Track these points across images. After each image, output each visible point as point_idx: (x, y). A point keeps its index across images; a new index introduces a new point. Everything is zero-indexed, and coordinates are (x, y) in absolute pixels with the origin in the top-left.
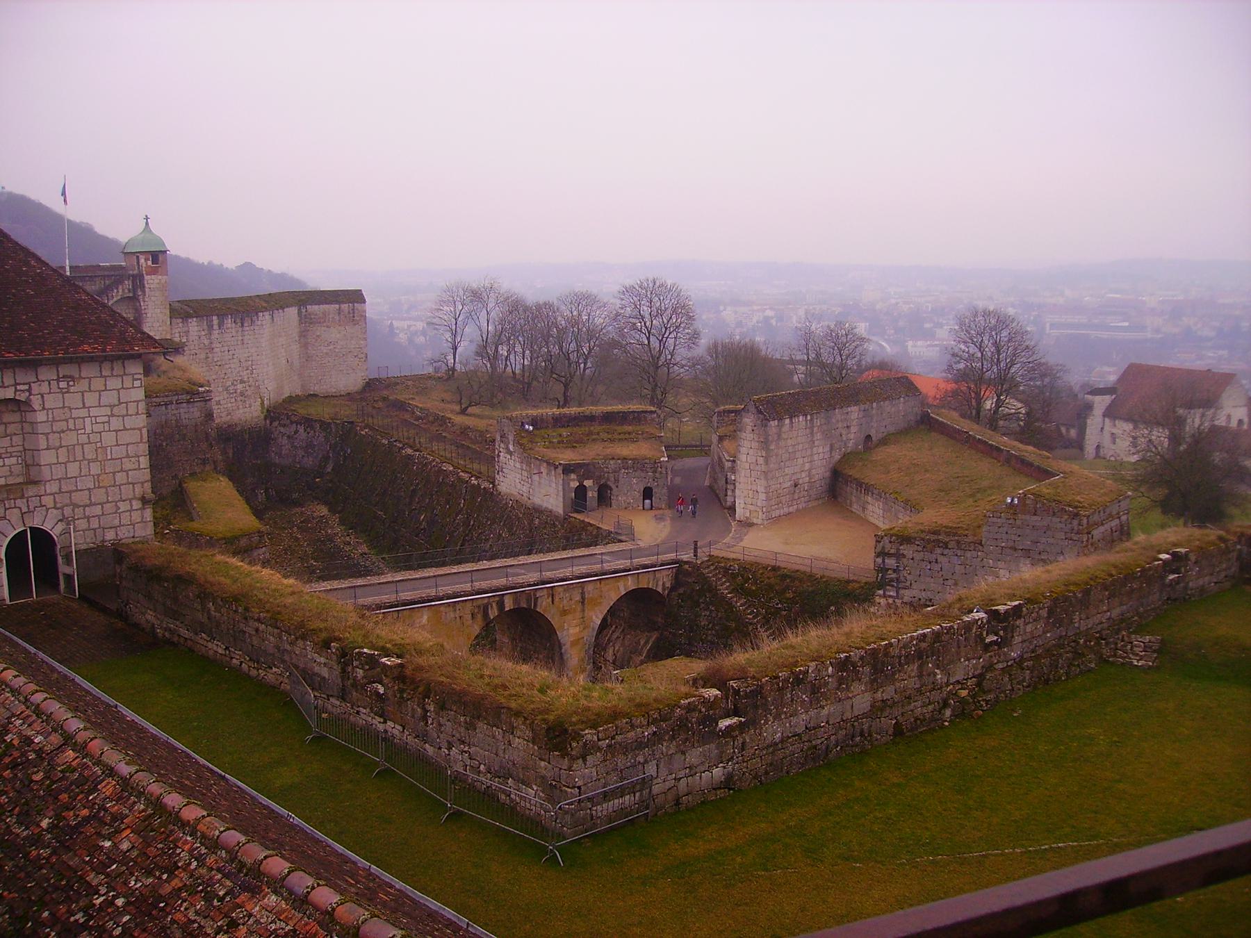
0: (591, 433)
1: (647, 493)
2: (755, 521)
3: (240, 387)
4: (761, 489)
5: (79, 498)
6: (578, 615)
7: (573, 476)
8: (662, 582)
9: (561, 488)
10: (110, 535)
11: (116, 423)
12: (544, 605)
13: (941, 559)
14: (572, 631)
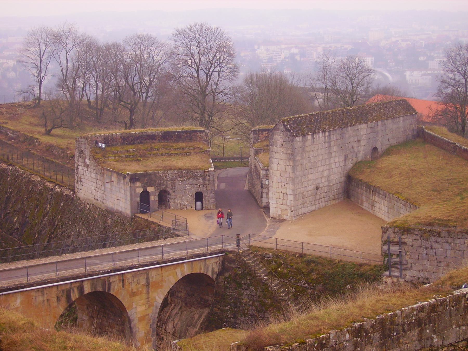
0: (152, 149)
1: (199, 197)
2: (285, 217)
4: (290, 192)
6: (144, 296)
7: (138, 184)
8: (211, 268)
9: (128, 193)
12: (116, 289)
13: (435, 245)
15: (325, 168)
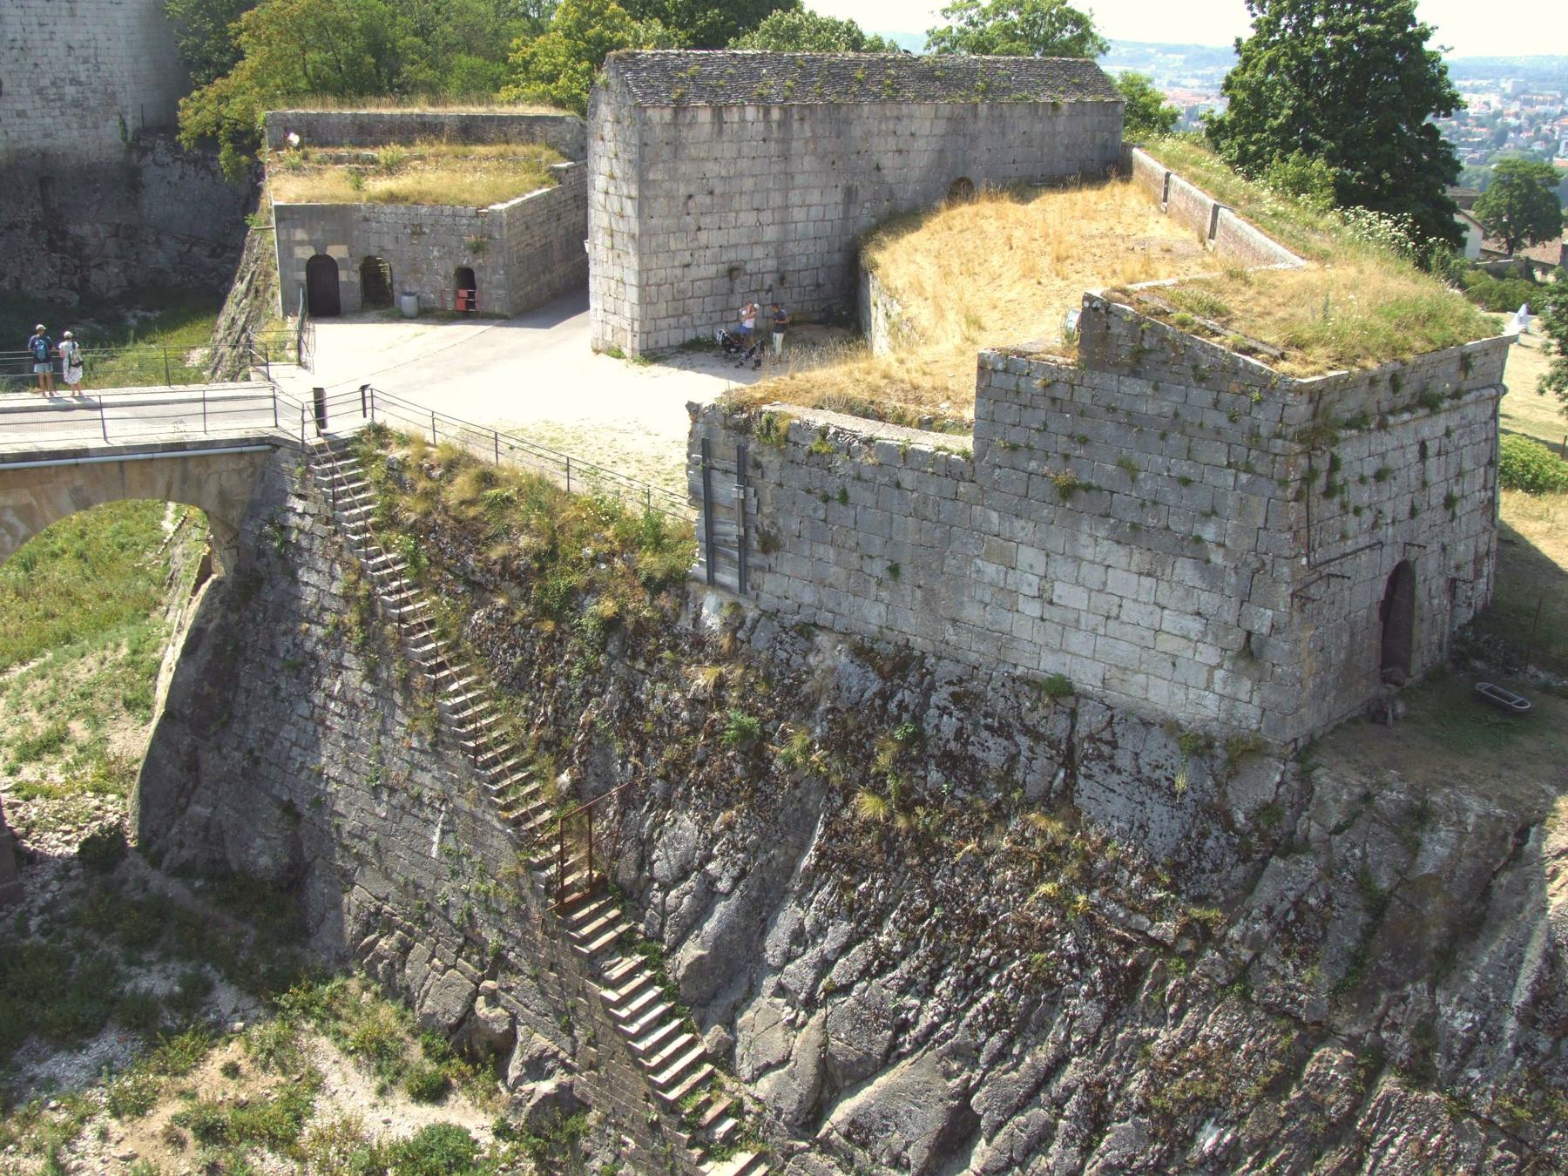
3: (70, 91)
4: (632, 279)
15: (766, 217)
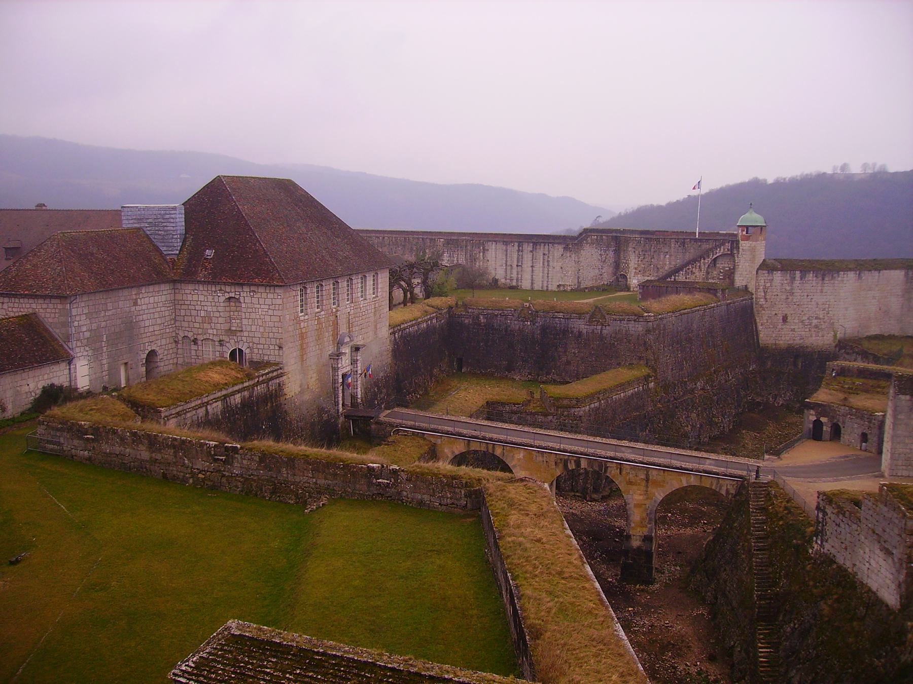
0: (879, 387)
3: (815, 322)
5: (256, 340)
6: (643, 488)
7: (812, 412)
10: (266, 358)
11: (270, 312)
12: (612, 472)
14: (637, 497)
